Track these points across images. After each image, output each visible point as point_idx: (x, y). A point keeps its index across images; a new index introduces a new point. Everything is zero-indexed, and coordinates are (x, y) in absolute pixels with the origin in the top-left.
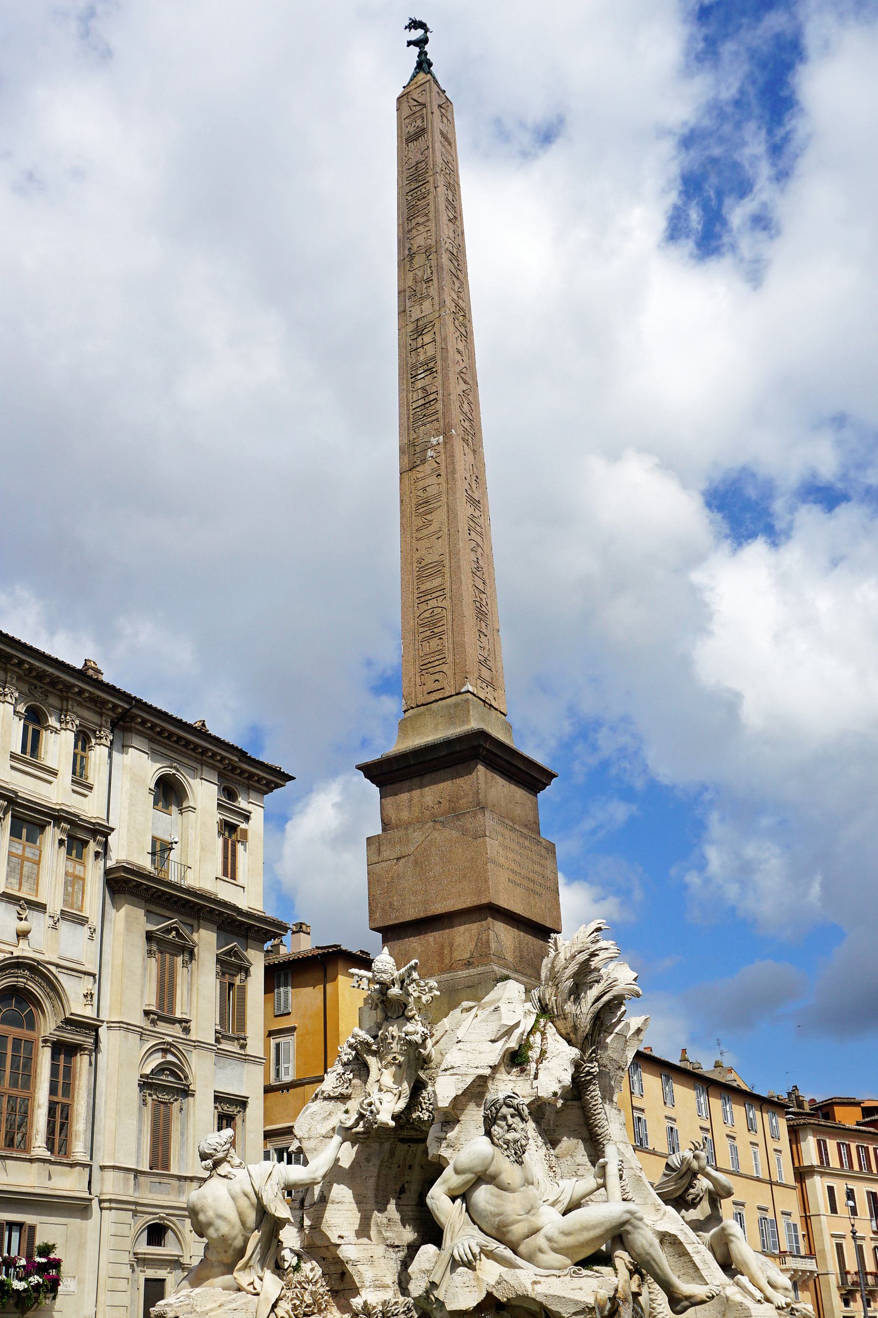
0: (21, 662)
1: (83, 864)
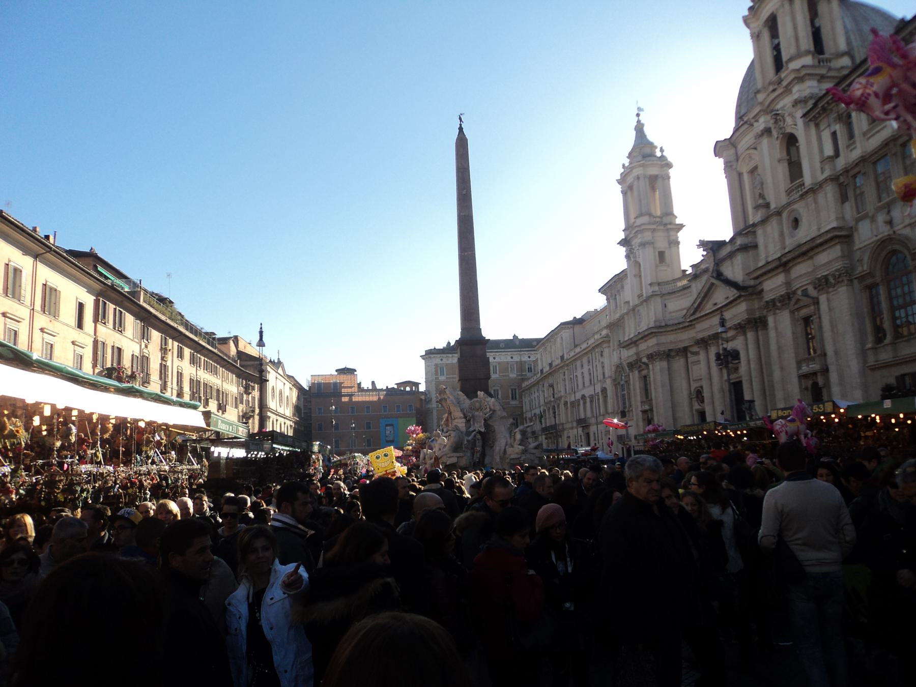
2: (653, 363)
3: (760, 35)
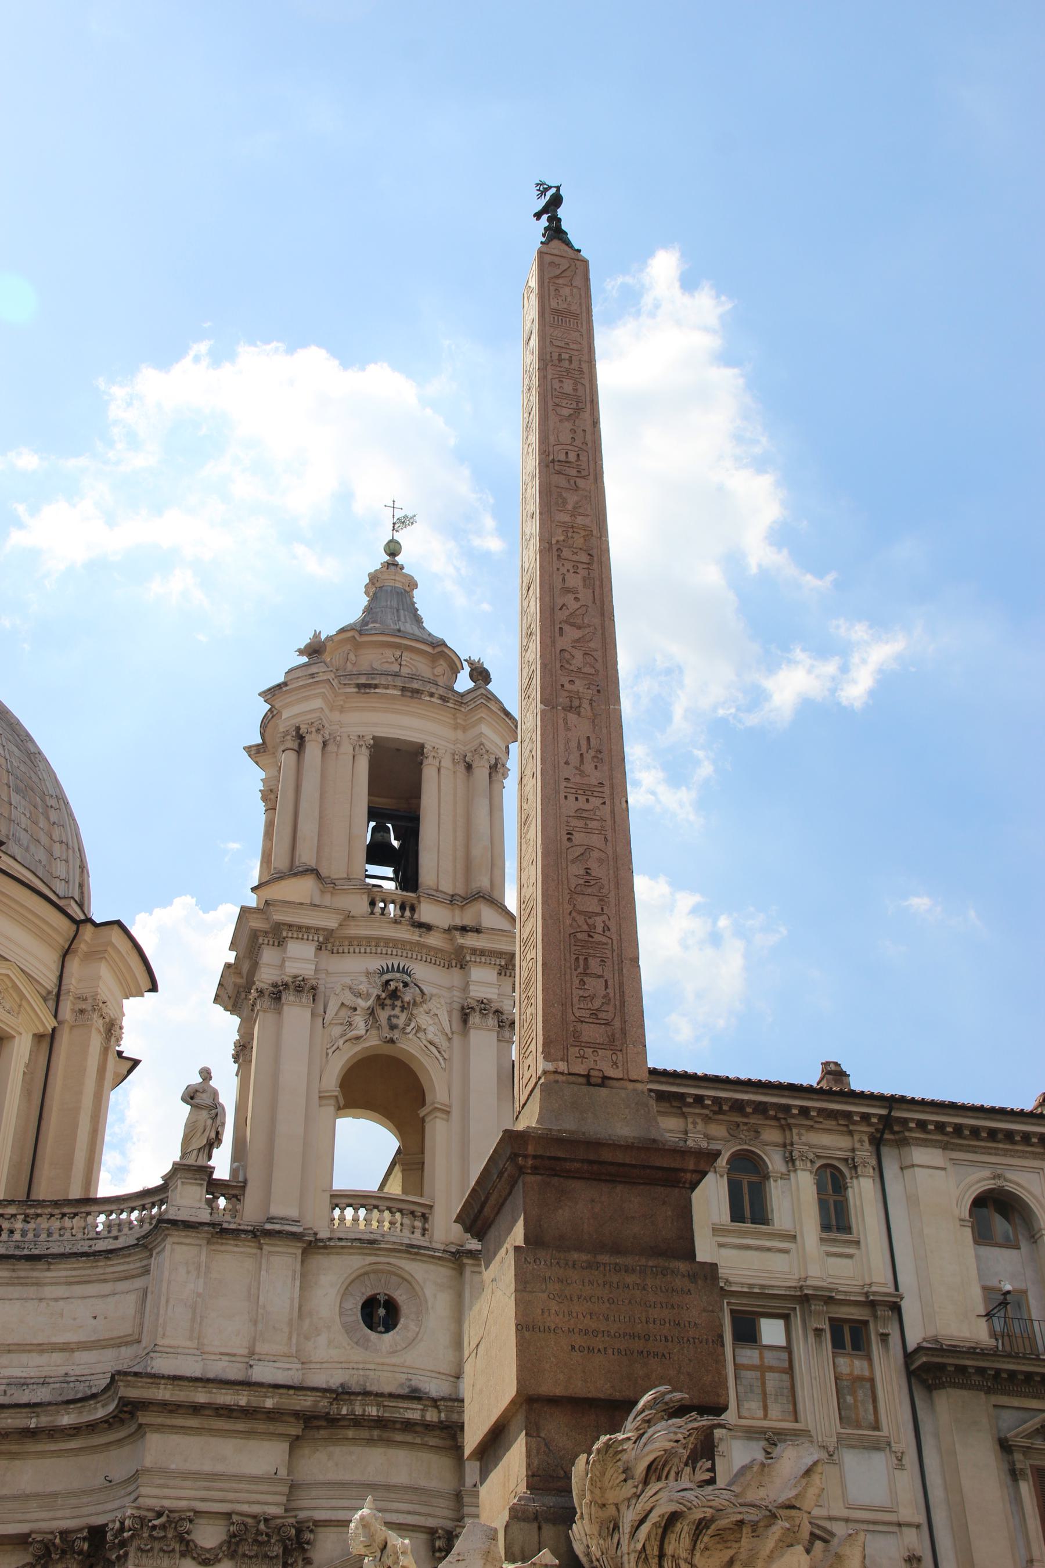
0: (699, 1100)
1: (869, 1358)
3: (331, 747)
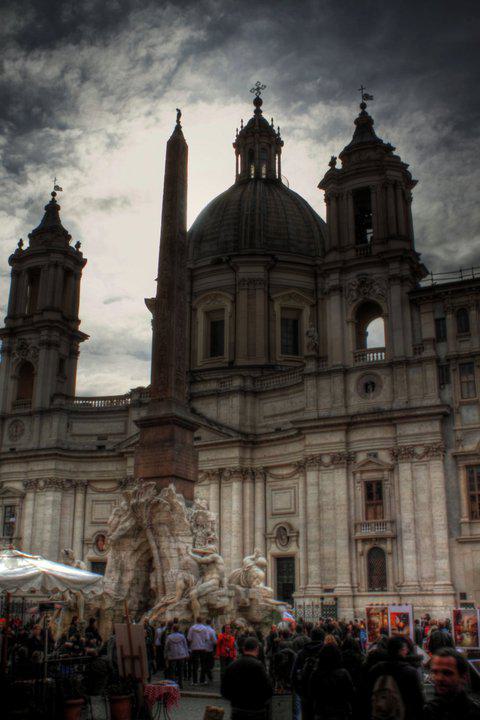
2: (36, 492)
